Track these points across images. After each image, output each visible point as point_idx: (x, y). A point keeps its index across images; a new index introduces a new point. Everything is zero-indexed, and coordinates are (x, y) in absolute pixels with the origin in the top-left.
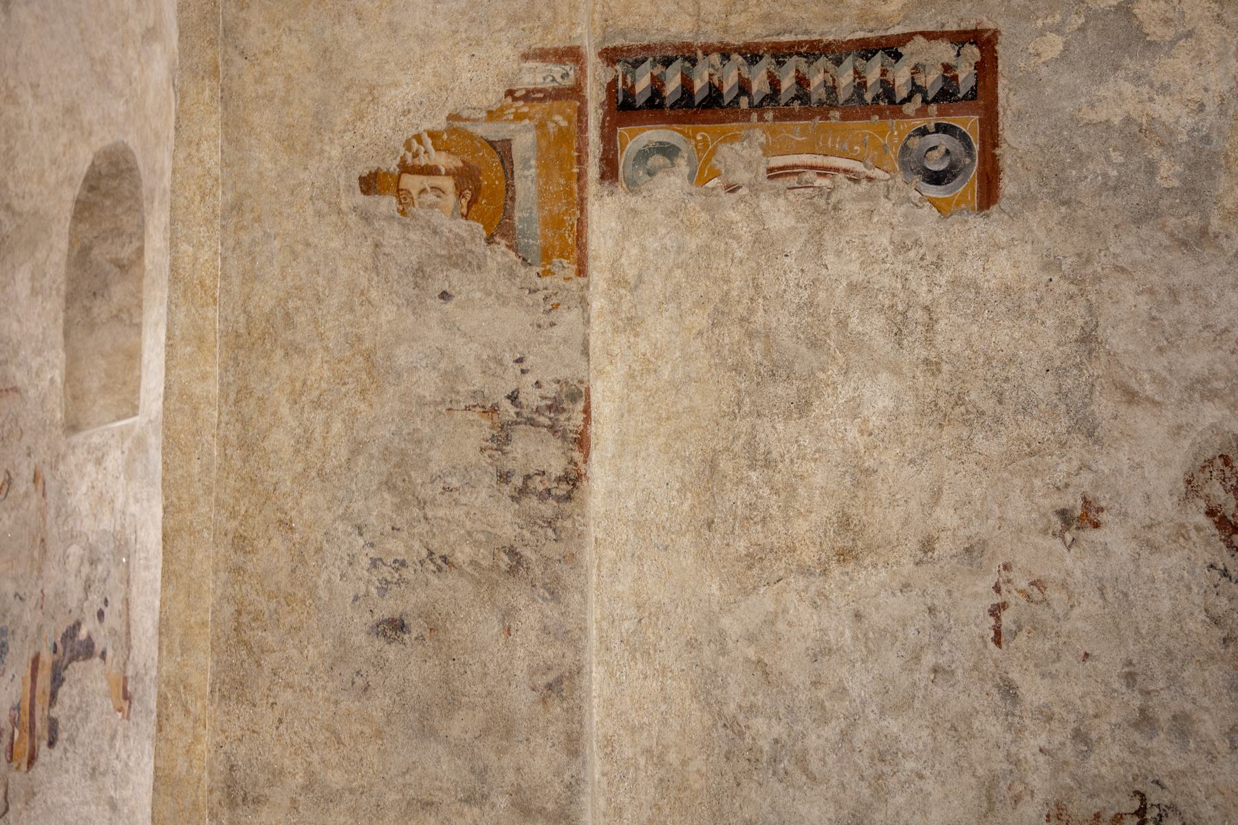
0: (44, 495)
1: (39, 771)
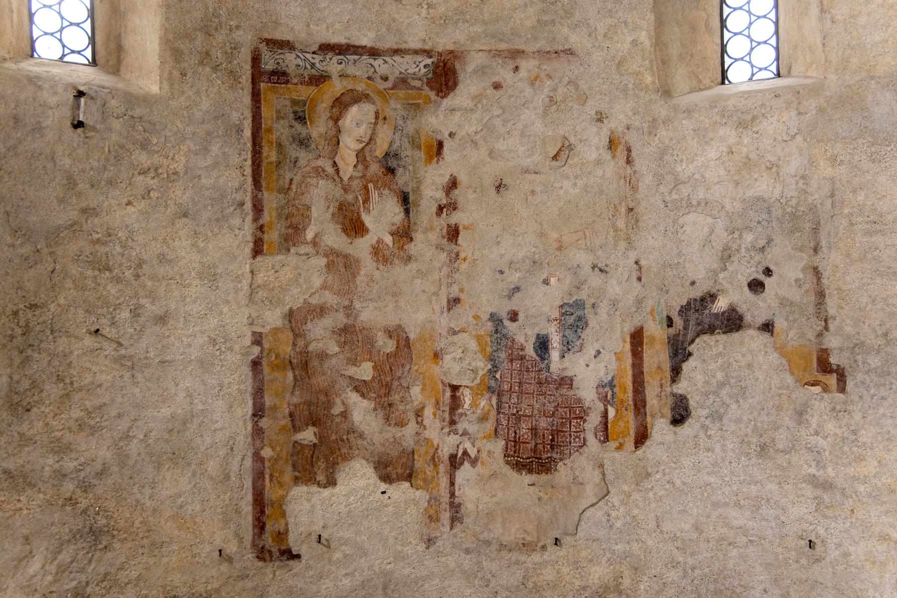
0: (629, 161)
1: (650, 449)
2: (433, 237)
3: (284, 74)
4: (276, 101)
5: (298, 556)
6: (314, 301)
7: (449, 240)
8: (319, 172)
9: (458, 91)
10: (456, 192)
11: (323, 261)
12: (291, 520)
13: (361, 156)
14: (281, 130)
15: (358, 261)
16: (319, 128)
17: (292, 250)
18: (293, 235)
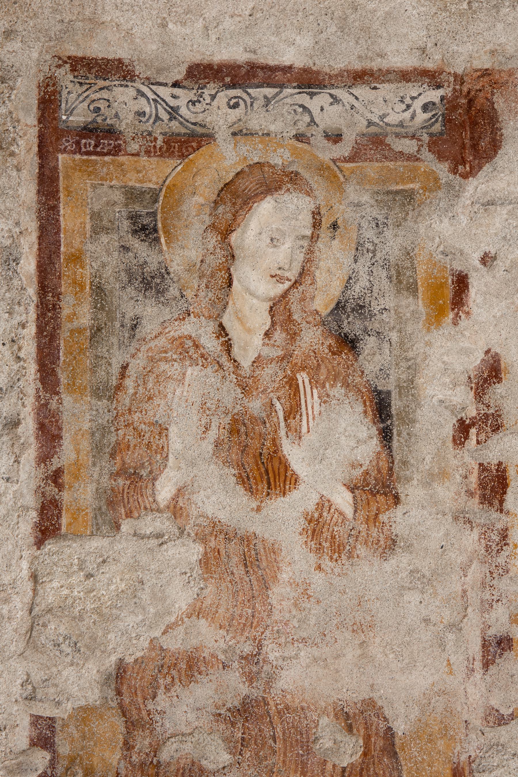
2: (448, 493)
3: (111, 132)
4: (93, 193)
6: (174, 643)
7: (485, 500)
8: (187, 349)
9: (500, 160)
10: (499, 389)
11: (195, 551)
13: (280, 311)
14: (103, 256)
15: (274, 550)
16: (186, 251)
17: (126, 526)
18: (127, 491)
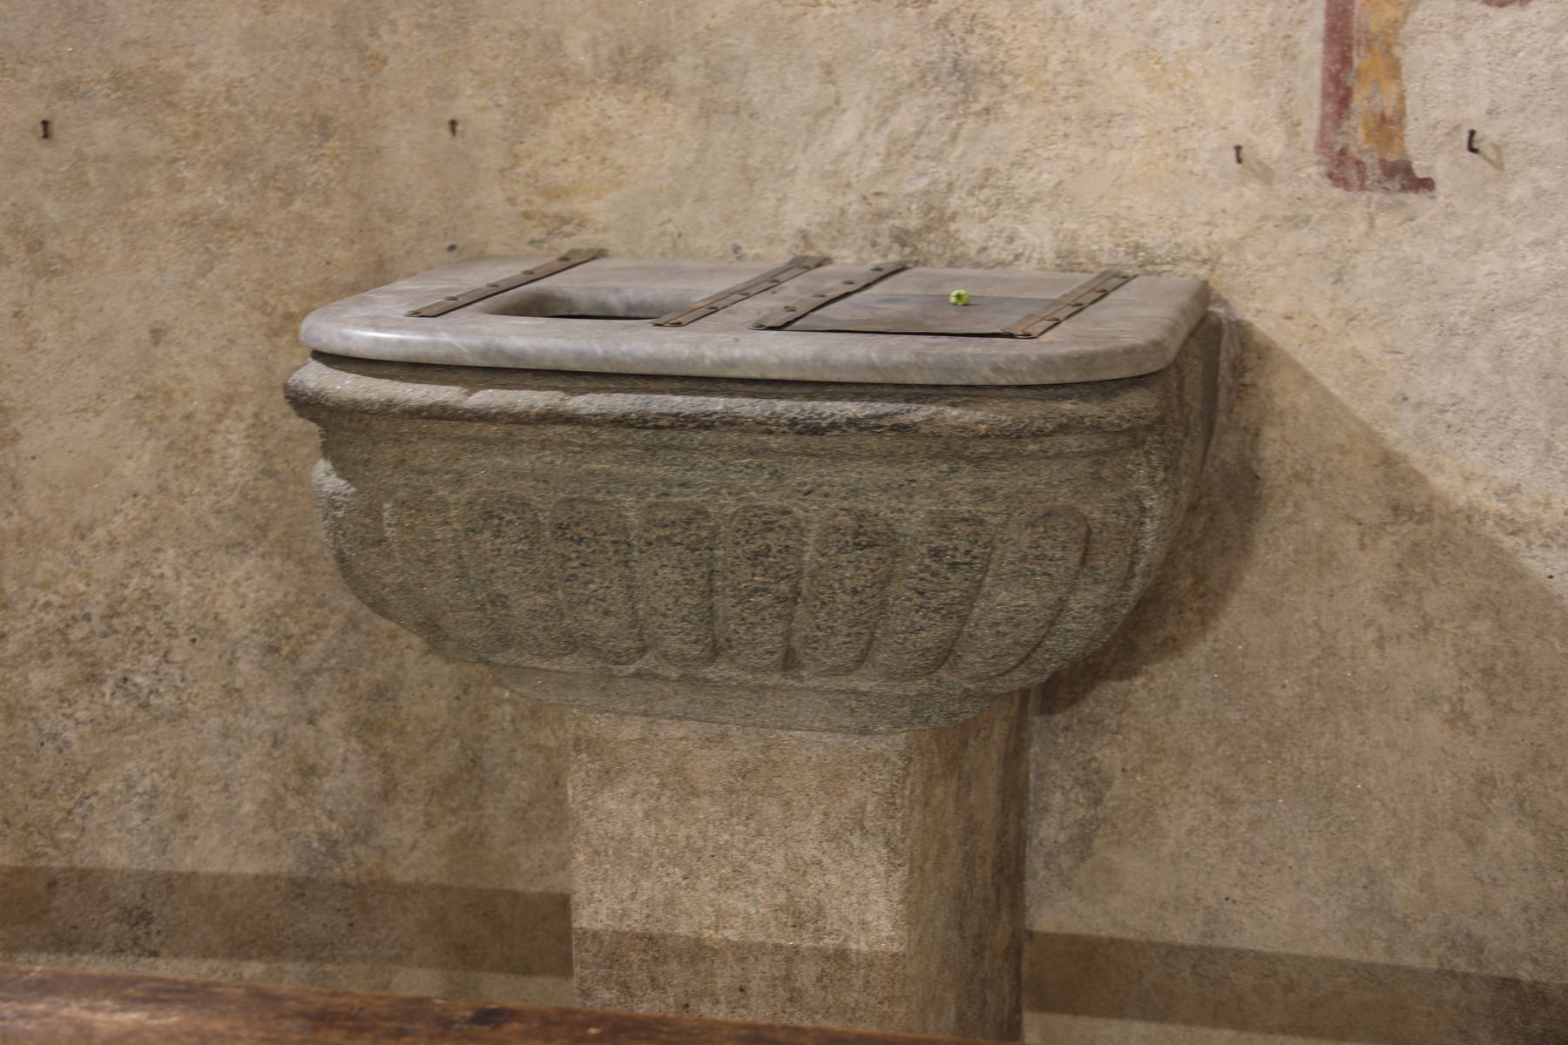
5: (1426, 184)
12: (1413, 88)
